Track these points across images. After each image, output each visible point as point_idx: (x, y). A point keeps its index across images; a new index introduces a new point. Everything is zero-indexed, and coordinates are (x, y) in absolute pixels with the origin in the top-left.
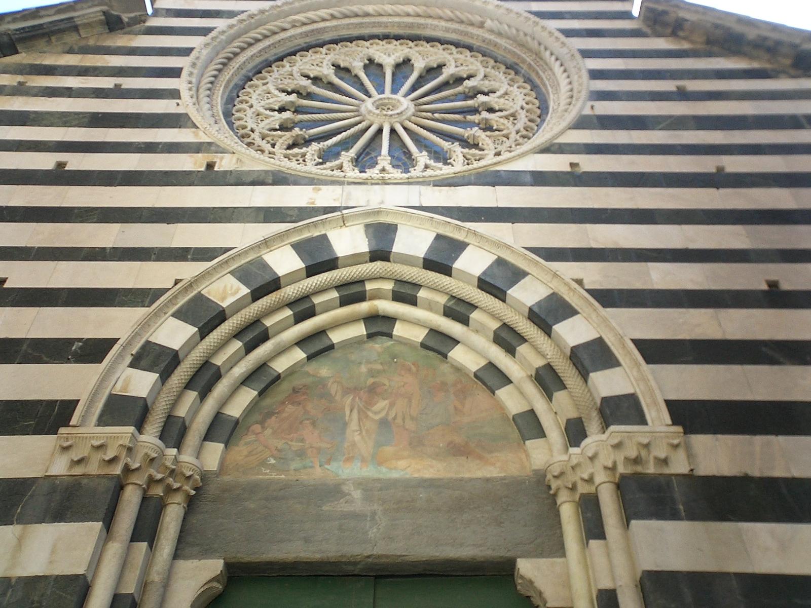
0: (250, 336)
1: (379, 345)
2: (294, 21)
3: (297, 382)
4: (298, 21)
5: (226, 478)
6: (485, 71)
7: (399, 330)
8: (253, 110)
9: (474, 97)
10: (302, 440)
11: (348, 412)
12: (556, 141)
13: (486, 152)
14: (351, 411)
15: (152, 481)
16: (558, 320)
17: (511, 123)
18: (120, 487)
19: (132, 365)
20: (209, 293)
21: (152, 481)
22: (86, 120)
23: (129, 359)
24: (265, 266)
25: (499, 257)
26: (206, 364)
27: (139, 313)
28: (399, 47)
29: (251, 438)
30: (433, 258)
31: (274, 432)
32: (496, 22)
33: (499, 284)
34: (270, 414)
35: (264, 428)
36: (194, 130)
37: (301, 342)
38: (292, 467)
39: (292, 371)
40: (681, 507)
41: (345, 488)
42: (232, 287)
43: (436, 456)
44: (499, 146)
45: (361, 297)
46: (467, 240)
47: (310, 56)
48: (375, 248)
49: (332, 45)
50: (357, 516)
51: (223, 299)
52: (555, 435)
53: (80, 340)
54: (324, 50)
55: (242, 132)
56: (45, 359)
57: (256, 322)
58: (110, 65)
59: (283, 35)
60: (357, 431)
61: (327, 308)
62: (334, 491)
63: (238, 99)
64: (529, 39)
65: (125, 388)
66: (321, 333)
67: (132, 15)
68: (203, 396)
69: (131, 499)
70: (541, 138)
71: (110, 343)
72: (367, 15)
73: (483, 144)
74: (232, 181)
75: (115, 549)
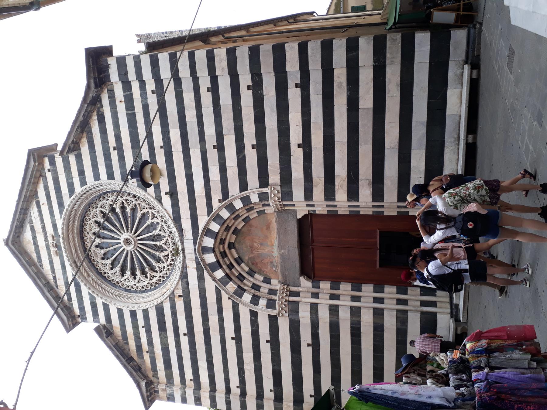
0: (242, 279)
1: (237, 245)
2: (87, 277)
3: (250, 264)
4: (87, 275)
5: (280, 278)
8: (137, 284)
9: (117, 214)
10: (268, 262)
11: (258, 252)
12: (155, 197)
13: (150, 212)
15: (286, 296)
17: (131, 202)
19: (258, 305)
21: (286, 296)
22: (163, 332)
23: (256, 306)
24: (221, 278)
26: (252, 287)
27: (241, 307)
28: (88, 237)
30: (214, 237)
31: (266, 269)
32: (75, 206)
33: (223, 221)
34: (260, 270)
35: (265, 271)
36: (163, 303)
37: (239, 264)
41: (281, 254)
43: (270, 233)
45: (225, 251)
47: (100, 267)
48: (212, 252)
50: (288, 251)
51: (235, 287)
53: (251, 318)
54: (95, 263)
57: (237, 277)
58: (132, 331)
59: (96, 279)
62: (282, 256)
63: (132, 289)
64: (85, 195)
65: (265, 306)
66: (235, 260)
67: (102, 329)
68: (260, 287)
69: (292, 299)
70: (155, 203)
71: (251, 311)
72: (76, 251)
74: (187, 290)
75: (303, 300)
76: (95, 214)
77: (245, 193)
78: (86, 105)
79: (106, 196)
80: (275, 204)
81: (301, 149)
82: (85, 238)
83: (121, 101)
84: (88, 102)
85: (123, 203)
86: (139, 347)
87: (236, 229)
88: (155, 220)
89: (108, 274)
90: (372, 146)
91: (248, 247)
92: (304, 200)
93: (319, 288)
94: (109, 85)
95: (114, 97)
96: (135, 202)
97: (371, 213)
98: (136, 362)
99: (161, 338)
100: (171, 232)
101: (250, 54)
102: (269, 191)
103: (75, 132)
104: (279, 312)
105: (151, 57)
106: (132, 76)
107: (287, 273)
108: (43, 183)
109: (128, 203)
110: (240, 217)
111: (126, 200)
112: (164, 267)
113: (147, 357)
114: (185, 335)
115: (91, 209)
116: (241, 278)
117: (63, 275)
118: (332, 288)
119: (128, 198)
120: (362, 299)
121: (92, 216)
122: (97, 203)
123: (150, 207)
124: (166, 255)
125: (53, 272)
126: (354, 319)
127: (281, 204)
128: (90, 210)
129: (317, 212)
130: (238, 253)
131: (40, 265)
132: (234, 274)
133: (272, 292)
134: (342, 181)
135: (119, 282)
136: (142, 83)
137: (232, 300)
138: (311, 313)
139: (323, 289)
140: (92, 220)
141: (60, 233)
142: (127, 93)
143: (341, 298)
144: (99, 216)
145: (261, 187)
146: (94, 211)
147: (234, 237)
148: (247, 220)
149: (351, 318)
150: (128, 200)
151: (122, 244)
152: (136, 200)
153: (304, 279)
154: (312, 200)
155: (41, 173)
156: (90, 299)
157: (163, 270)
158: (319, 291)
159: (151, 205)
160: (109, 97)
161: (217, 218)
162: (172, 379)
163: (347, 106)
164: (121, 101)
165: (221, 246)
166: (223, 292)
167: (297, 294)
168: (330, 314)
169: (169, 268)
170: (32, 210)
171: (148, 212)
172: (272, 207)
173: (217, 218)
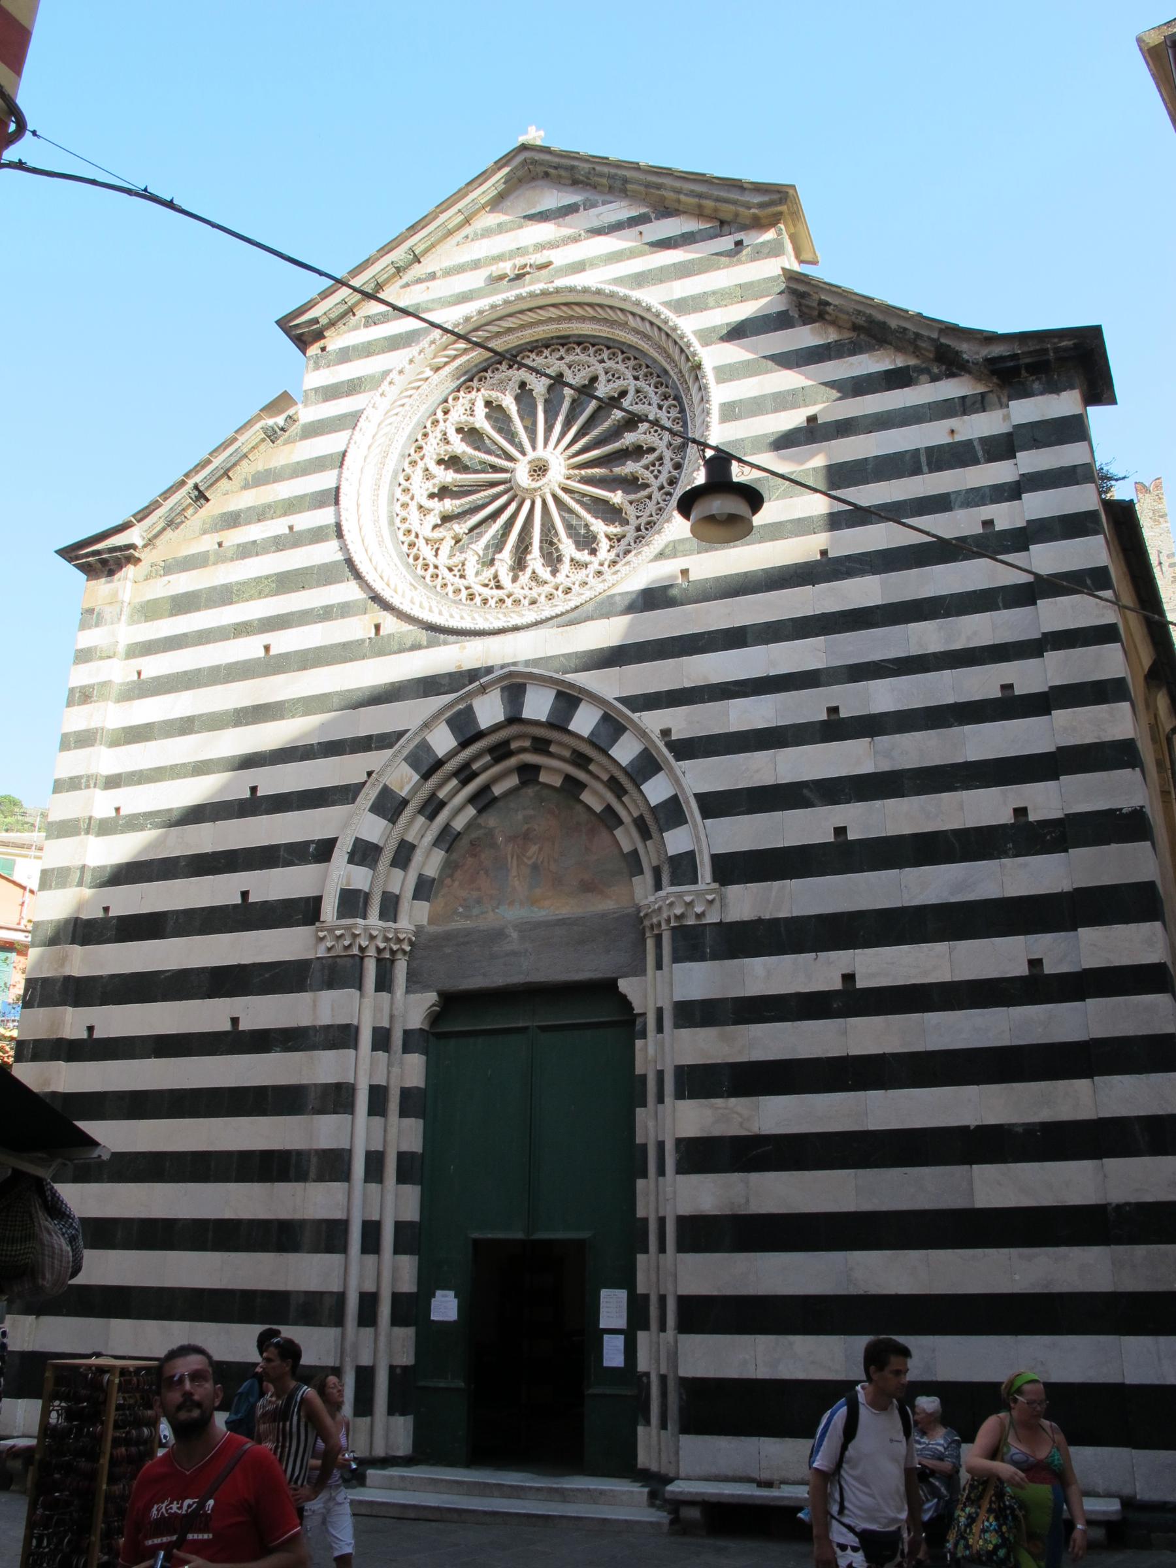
1: (530, 791)
3: (474, 835)
5: (432, 929)
6: (635, 385)
7: (543, 778)
10: (479, 889)
11: (509, 860)
14: (512, 858)
15: (379, 951)
16: (646, 778)
17: (656, 472)
18: (362, 958)
19: (350, 861)
20: (391, 783)
21: (379, 951)
22: (274, 585)
23: (346, 857)
25: (605, 712)
28: (549, 360)
29: (444, 891)
30: (551, 721)
33: (603, 745)
35: (453, 881)
37: (472, 800)
38: (475, 914)
39: (470, 825)
40: (708, 950)
42: (406, 776)
44: (641, 514)
45: (510, 754)
46: (580, 696)
49: (482, 374)
50: (514, 953)
51: (402, 788)
52: (648, 876)
53: (312, 842)
55: (407, 540)
56: (296, 862)
57: (433, 795)
58: (280, 498)
60: (515, 877)
61: (485, 768)
62: (497, 935)
66: (486, 789)
73: (626, 513)
74: (396, 648)
76: (616, 376)
77: (693, 809)
78: (935, 335)
79: (671, 402)
80: (660, 909)
81: (837, 985)
82: (546, 352)
83: (952, 431)
84: (943, 340)
85: (652, 450)
86: (233, 520)
87: (582, 786)
88: (604, 544)
89: (445, 422)
90: (852, 1209)
91: (526, 827)
92: (677, 998)
93: (406, 1049)
94: (999, 398)
95: (965, 413)
96: (655, 484)
97: (640, 1213)
98: (192, 515)
99: (258, 580)
100: (568, 591)
101: (1124, 811)
102: (701, 886)
103: (857, 310)
104: (331, 930)
105: (1092, 515)
106: (1030, 461)
107: (448, 950)
108: (701, 230)
109: (654, 465)
110: (619, 798)
111: (660, 458)
112: (462, 576)
113: (208, 543)
114: (267, 648)
115: (632, 363)
116: (432, 807)
117: (440, 298)
118: (405, 1093)
119: (668, 465)
120: (373, 1187)
121: (610, 368)
122: (649, 378)
123: (642, 527)
124: (498, 581)
125: (449, 272)
126: (314, 1160)
127: (664, 926)
128: (629, 359)
129: (639, 1043)
130: (507, 794)
131: (467, 237)
132: (441, 785)
133: (390, 907)
134: (740, 1120)
135: (421, 454)
136: (1013, 491)
137: (366, 781)
138: (328, 1028)
139: (401, 1064)
140: (599, 369)
141: (561, 282)
142: (978, 448)
143: (377, 1120)
144: (611, 385)
145: (715, 858)
146: (626, 371)
147: (557, 781)
148: (610, 818)
149: (317, 1152)
150: (661, 465)
151: (531, 455)
152: (661, 488)
153: (431, 1004)
154: (678, 1025)
155: (729, 223)
156: (372, 377)
157: (455, 575)
158: (395, 1053)
159: (647, 529)
160: (963, 398)
161: (612, 726)
162: (143, 618)
163: (980, 1128)
164: (952, 431)
165: (527, 743)
166: (388, 753)
167: (384, 983)
168: (326, 1086)
169: (460, 590)
170: (623, 204)
171: (627, 523)
172: (652, 899)
173: (612, 726)
